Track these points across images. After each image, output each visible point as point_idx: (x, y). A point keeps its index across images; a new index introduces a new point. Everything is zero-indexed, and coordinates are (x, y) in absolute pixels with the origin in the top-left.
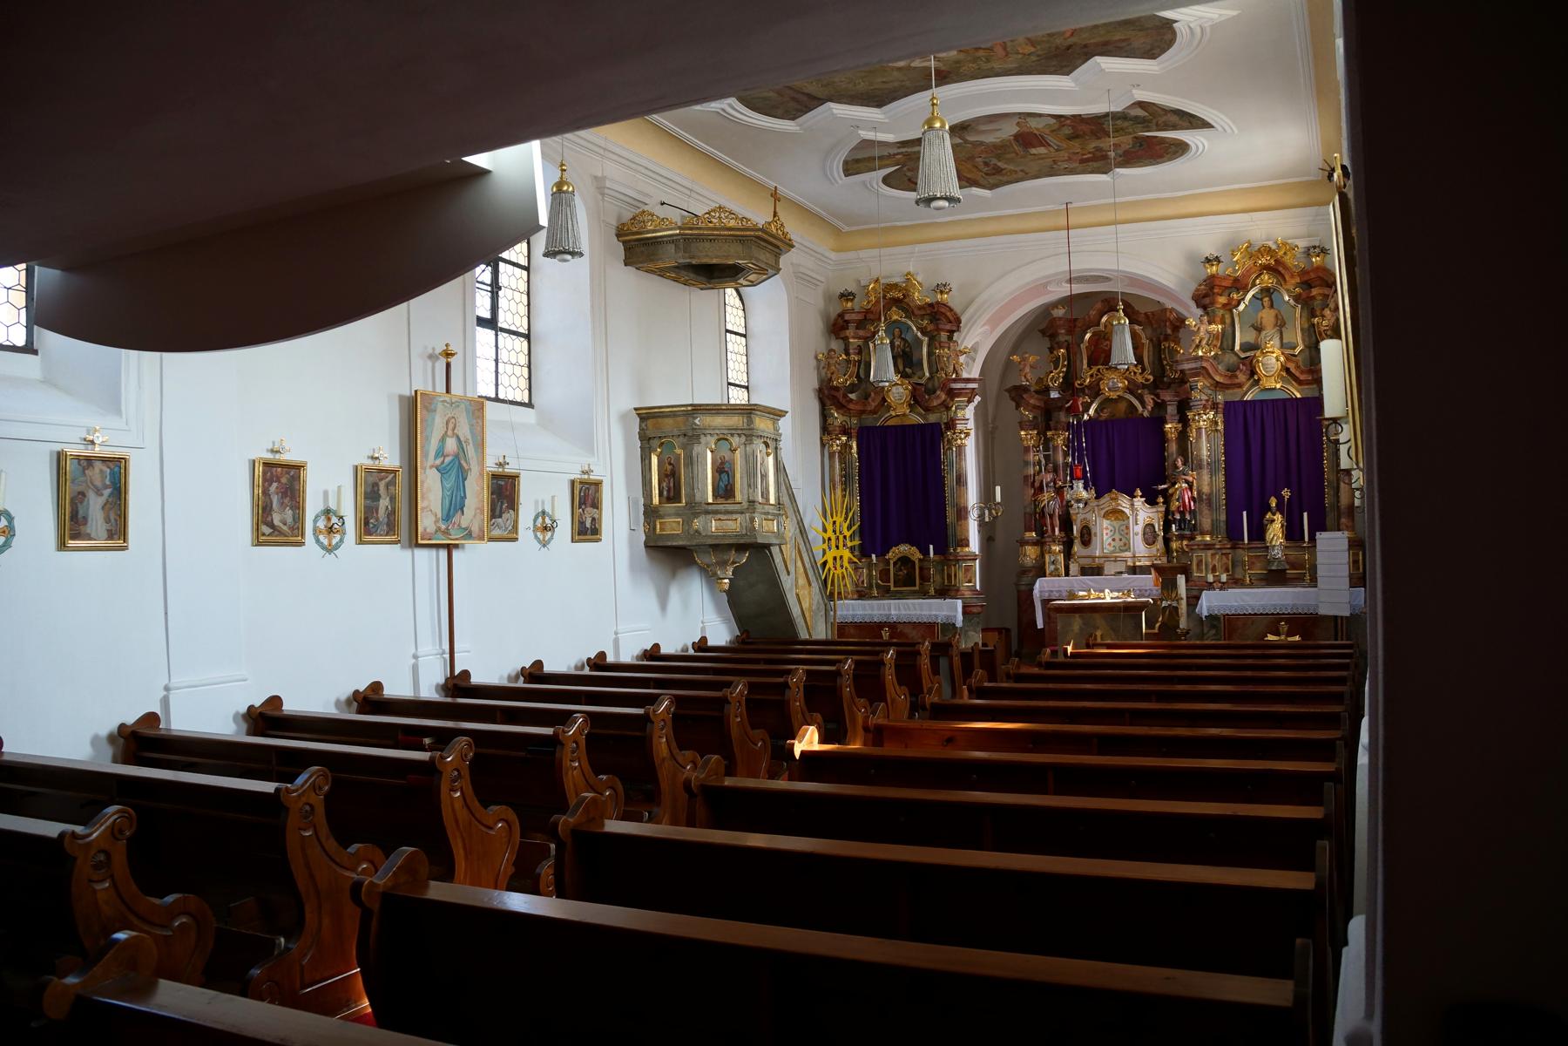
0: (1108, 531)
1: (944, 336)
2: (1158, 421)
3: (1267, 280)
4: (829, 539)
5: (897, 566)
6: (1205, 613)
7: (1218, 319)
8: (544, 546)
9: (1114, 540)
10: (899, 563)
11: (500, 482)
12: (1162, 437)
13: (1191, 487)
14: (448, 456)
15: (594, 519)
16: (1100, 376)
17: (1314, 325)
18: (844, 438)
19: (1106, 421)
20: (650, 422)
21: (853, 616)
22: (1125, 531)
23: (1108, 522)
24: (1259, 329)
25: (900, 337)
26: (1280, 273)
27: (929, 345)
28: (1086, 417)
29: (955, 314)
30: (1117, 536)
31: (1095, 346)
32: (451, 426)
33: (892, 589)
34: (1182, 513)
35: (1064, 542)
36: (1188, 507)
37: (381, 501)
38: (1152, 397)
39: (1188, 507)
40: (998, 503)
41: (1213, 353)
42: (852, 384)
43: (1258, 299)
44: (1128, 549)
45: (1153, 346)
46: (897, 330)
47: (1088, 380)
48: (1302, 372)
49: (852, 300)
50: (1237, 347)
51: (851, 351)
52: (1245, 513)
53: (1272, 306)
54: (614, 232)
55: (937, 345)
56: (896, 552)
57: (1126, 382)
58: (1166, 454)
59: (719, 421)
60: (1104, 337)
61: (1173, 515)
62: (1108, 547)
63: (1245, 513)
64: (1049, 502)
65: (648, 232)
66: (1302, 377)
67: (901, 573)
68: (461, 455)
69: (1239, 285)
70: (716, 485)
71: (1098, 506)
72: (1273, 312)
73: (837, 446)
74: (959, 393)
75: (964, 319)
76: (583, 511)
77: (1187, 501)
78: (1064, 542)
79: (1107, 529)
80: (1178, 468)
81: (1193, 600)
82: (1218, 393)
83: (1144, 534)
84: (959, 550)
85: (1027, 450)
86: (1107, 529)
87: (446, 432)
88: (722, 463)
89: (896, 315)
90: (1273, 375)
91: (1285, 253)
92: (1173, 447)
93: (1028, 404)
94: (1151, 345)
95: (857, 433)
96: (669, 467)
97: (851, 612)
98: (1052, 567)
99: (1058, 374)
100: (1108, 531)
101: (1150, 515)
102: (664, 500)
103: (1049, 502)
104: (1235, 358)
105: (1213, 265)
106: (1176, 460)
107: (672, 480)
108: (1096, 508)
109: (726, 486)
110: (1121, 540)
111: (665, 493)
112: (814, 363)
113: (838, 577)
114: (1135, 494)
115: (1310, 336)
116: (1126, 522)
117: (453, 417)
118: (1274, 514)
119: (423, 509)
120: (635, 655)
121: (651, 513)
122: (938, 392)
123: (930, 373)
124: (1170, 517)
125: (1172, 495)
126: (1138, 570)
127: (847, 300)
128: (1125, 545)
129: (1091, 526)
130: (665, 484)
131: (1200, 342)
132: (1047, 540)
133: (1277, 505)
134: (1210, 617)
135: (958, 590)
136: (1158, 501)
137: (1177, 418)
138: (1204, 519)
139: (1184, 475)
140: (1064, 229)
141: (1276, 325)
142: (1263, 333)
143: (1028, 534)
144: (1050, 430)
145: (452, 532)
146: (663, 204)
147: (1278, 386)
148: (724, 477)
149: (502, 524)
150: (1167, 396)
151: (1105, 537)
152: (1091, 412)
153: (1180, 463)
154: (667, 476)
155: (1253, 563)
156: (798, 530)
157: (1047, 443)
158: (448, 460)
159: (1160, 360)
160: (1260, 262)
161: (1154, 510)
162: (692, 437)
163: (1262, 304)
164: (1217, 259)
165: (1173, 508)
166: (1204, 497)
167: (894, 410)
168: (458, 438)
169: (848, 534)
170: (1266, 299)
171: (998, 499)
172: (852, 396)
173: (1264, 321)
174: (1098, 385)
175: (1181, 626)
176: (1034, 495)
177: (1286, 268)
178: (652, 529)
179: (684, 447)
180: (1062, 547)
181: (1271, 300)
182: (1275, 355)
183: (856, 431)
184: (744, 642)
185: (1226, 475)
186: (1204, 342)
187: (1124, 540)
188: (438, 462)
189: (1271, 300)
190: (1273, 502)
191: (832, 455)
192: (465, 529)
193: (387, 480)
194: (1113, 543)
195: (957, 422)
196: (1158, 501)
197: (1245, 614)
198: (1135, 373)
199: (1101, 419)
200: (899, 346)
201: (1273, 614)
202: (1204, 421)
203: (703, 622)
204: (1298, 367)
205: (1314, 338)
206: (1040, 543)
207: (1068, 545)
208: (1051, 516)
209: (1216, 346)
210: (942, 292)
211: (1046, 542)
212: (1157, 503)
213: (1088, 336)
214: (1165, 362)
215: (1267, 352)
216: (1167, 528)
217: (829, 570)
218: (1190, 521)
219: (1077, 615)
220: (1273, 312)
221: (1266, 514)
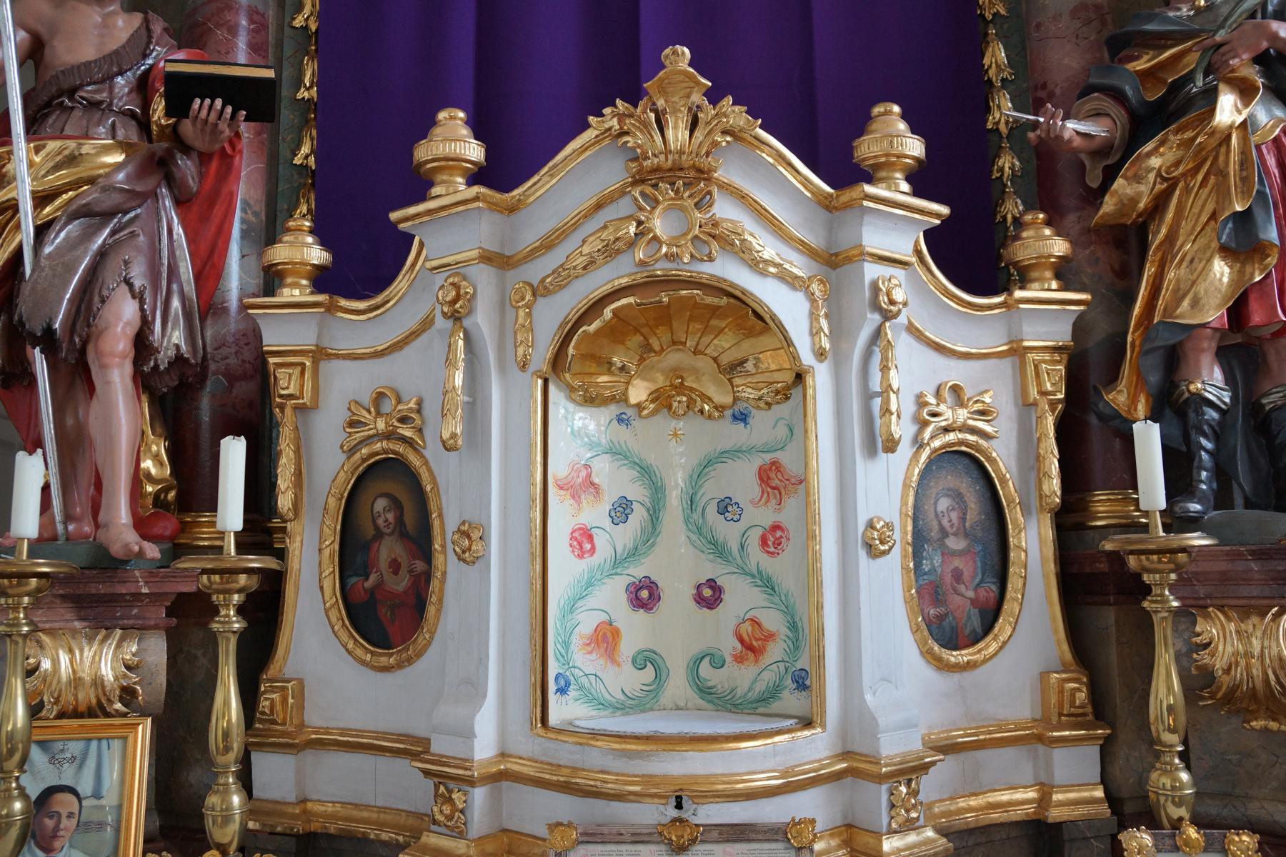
0: (595, 514)
22: (766, 517)
62: (585, 662)
71: (498, 260)
79: (585, 486)
83: (919, 541)
86: (585, 486)
108: (484, 281)
110: (709, 595)
114: (867, 148)
116: (764, 426)
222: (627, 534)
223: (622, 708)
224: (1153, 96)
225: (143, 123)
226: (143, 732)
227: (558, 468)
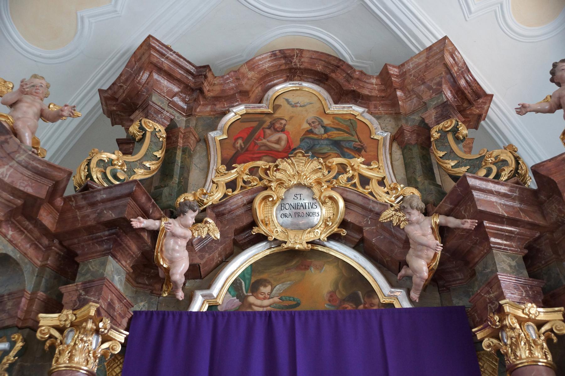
19: (268, 316)
31: (246, 141)
38: (438, 219)
45: (404, 147)
57: (341, 204)
94: (395, 145)
198: (365, 181)
213: (230, 117)
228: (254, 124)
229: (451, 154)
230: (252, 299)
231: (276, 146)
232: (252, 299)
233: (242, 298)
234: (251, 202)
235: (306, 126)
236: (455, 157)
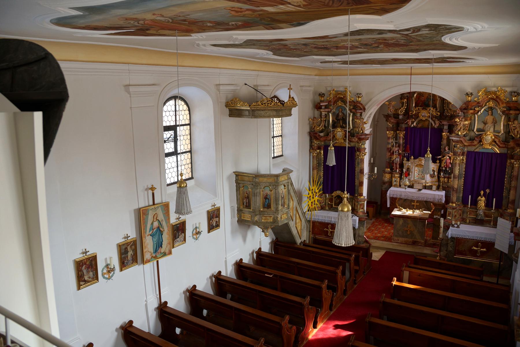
1: (358, 115)
2: (440, 130)
3: (491, 104)
4: (310, 196)
5: (336, 198)
6: (450, 236)
7: (469, 119)
8: (197, 239)
9: (419, 175)
10: (337, 198)
11: (177, 226)
12: (441, 137)
13: (450, 158)
14: (154, 229)
15: (217, 222)
16: (419, 111)
17: (509, 125)
18: (318, 151)
19: (420, 128)
20: (239, 177)
21: (318, 219)
23: (417, 168)
24: (485, 123)
25: (342, 112)
26: (497, 101)
27: (353, 116)
28: (412, 126)
29: (363, 106)
30: (420, 173)
32: (155, 217)
33: (333, 206)
34: (446, 168)
35: (400, 173)
36: (448, 166)
37: (129, 253)
39: (448, 166)
40: (375, 174)
41: (465, 133)
42: (323, 129)
43: (486, 111)
44: (424, 179)
45: (441, 100)
46: (341, 109)
47: (414, 112)
48: (501, 144)
49: (323, 97)
50: (475, 130)
51: (322, 117)
52: (470, 196)
53: (492, 115)
54: (224, 105)
55: (356, 118)
56: (335, 194)
58: (442, 143)
59: (265, 180)
60: (422, 96)
61: (442, 168)
62: (416, 177)
63: (470, 196)
64: (395, 159)
65: (238, 107)
66: (501, 146)
67: (337, 201)
68: (160, 226)
69: (479, 104)
70: (264, 203)
71: (414, 162)
72: (492, 117)
73: (316, 154)
74: (363, 139)
75: (366, 107)
76: (212, 221)
77: (448, 164)
78: (400, 173)
79: (417, 170)
80: (446, 150)
81: (446, 228)
82: (465, 148)
84: (359, 197)
85: (389, 138)
86: (417, 170)
87: (153, 220)
88: (267, 195)
89: (340, 103)
90: (489, 143)
91: (501, 94)
92: (444, 142)
93: (390, 121)
95: (323, 148)
96: (247, 195)
97: (317, 218)
98: (395, 183)
99: (403, 109)
100: (417, 171)
101: (433, 167)
102: (245, 206)
103: (395, 159)
104: (474, 134)
105: (469, 96)
106: (445, 147)
107: (247, 200)
108: (413, 163)
109: (268, 204)
110: (421, 175)
111: (245, 204)
112: (308, 122)
113: (315, 184)
115: (506, 128)
117: (156, 214)
118: (482, 198)
119: (145, 252)
120: (233, 263)
121: (239, 211)
122: (355, 138)
123: (353, 127)
124: (441, 168)
125: (443, 160)
126: (427, 187)
127: (322, 97)
128: (423, 177)
129: (411, 168)
130: (245, 201)
131: (460, 129)
132: (394, 173)
133: (483, 194)
134: (452, 238)
135: (357, 212)
136: (437, 162)
137: (448, 131)
138: (453, 198)
139: (448, 154)
140: (410, 75)
141: (493, 123)
142: (487, 125)
143: (387, 169)
144: (398, 131)
145: (158, 256)
146: (246, 84)
147: (490, 148)
148: (267, 200)
149: (179, 240)
150: (445, 123)
151: (416, 173)
152: (415, 124)
153: (447, 149)
154: (246, 198)
155: (471, 213)
156: (297, 203)
157: (396, 137)
158: (154, 230)
159: (443, 107)
160: (490, 97)
161: (435, 165)
162: (256, 185)
163: (488, 113)
164: (472, 94)
165: (442, 166)
166: (455, 189)
167: (338, 140)
168: (158, 220)
169: (317, 191)
170: (490, 112)
171: (376, 172)
172: (322, 134)
173: (488, 121)
174: (418, 114)
175: (440, 237)
176: (391, 155)
177: (500, 100)
178: (240, 216)
179: (252, 189)
180: (399, 175)
181: (492, 112)
182: (491, 136)
183: (323, 147)
184: (275, 244)
185: (464, 180)
186: (462, 129)
187: (423, 175)
188: (151, 233)
189: (492, 112)
190: (482, 193)
191: (313, 157)
192: (163, 253)
193: (131, 245)
194: (418, 176)
195: (362, 150)
196: (437, 162)
197: (465, 238)
199: (418, 127)
200: (341, 116)
201: (476, 240)
202: (458, 160)
203: (260, 239)
204: (499, 141)
205: (508, 130)
206: (391, 173)
207: (401, 174)
208: (396, 164)
209: (466, 130)
210: (359, 97)
211: (393, 173)
212: (437, 163)
214: (445, 108)
215: (488, 135)
216: (439, 173)
217: (310, 207)
218: (449, 171)
219: (402, 219)
220: (492, 117)
221: (479, 197)
222: (418, 172)
223: (418, 179)
224: (444, 155)
225: (398, 153)
226: (399, 178)
227: (416, 170)
228: (420, 95)
229: (445, 107)
230: (418, 125)
231: (422, 100)
232: (418, 125)
233: (417, 125)
234: (418, 114)
235: (427, 96)
236: (446, 108)
